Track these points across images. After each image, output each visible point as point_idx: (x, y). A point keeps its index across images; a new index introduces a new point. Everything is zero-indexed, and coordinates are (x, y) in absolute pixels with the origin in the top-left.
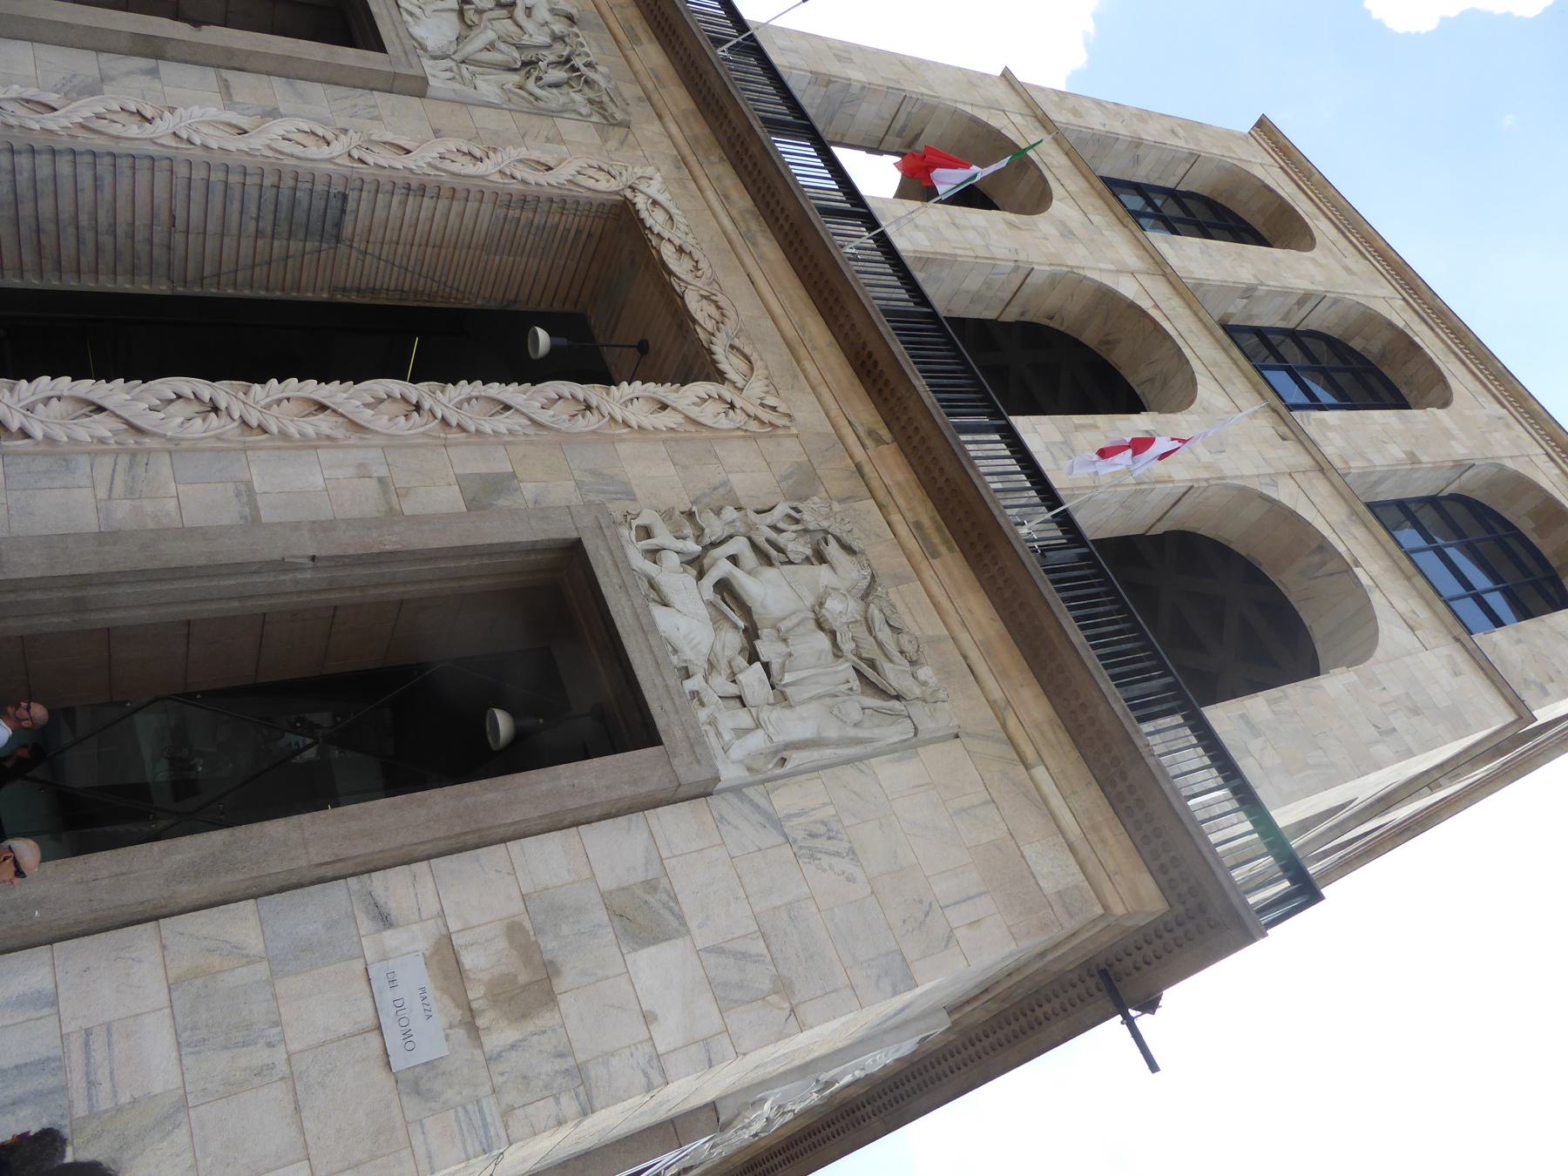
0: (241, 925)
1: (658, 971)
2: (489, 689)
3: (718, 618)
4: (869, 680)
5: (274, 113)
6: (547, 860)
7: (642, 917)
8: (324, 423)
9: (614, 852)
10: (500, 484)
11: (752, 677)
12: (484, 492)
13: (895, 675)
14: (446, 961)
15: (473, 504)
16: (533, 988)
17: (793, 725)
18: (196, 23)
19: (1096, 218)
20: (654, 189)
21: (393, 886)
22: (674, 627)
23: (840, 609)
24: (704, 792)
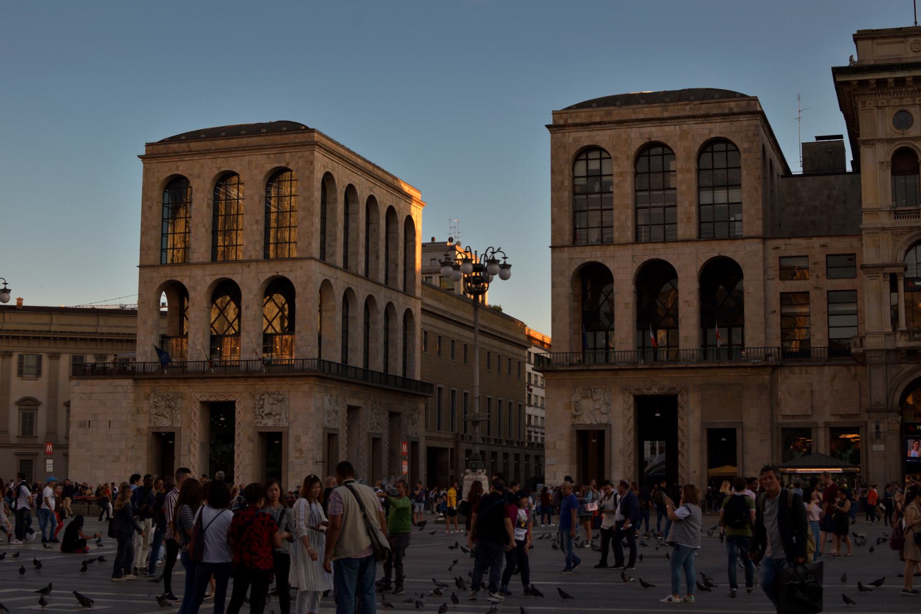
0: (290, 473)
1: (303, 439)
2: (272, 444)
3: (269, 418)
4: (281, 401)
5: (189, 451)
6: (291, 446)
7: (298, 439)
8: (241, 456)
9: (292, 440)
10: (249, 438)
11: (277, 417)
12: (250, 439)
13: (280, 398)
14: (297, 458)
15: (252, 441)
16: (301, 451)
17: (283, 416)
18: (174, 458)
19: (188, 273)
20: (198, 395)
21: (290, 460)
22: (269, 423)
23: (271, 401)
24: (288, 428)
